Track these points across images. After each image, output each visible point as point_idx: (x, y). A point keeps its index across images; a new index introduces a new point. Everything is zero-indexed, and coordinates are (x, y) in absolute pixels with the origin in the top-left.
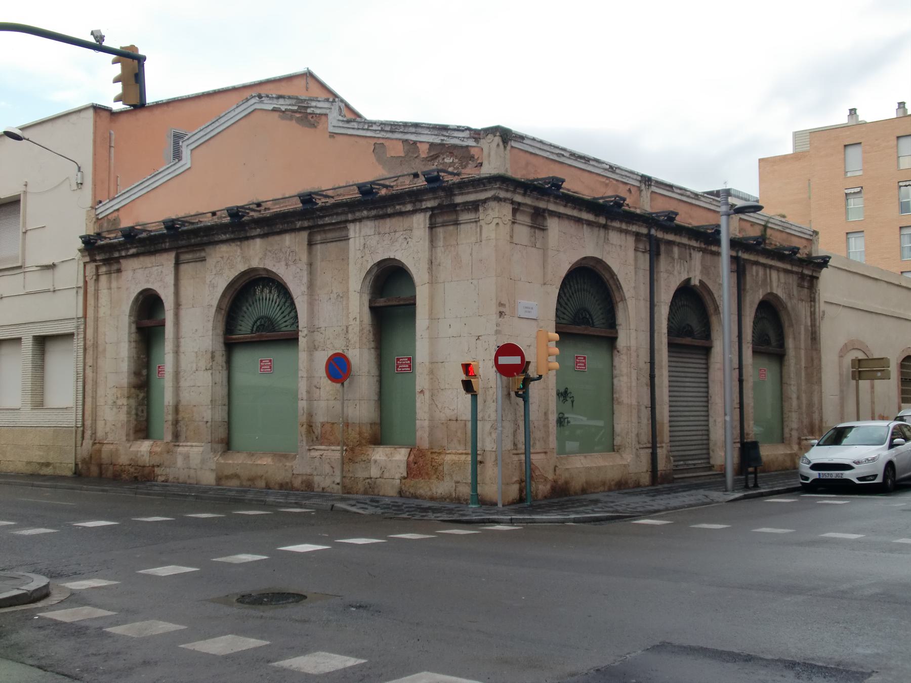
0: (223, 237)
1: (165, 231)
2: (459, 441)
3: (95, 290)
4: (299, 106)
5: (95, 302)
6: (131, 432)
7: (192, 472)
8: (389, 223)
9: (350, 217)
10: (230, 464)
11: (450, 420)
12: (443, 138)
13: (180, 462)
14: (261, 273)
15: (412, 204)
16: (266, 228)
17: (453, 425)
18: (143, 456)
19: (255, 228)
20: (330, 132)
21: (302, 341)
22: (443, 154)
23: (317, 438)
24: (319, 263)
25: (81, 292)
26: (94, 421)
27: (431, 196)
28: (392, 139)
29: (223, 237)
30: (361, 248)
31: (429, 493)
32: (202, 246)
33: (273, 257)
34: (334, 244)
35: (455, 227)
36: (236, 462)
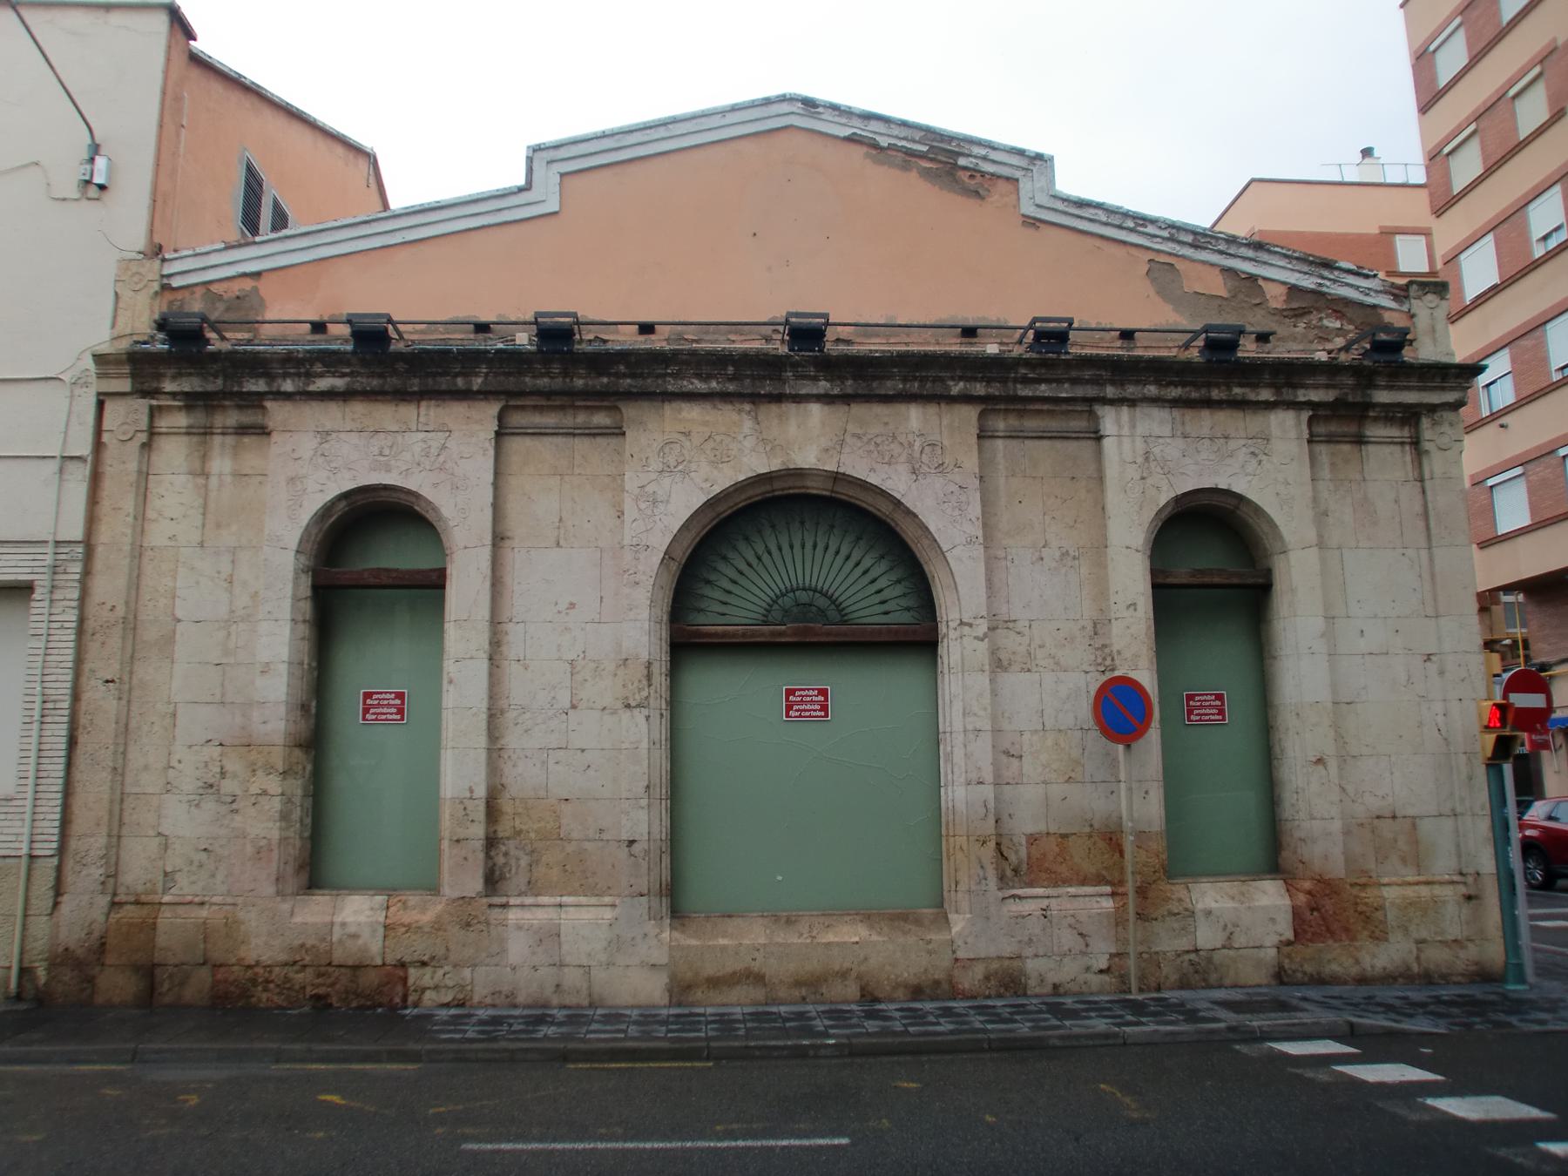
0: (699, 386)
1: (784, 350)
2: (1404, 860)
3: (140, 472)
4: (932, 147)
5: (136, 505)
6: (290, 869)
7: (572, 977)
8: (1206, 420)
9: (1110, 391)
10: (724, 948)
11: (1378, 817)
12: (1319, 281)
13: (518, 949)
14: (809, 484)
15: (1273, 390)
16: (850, 382)
17: (1386, 828)
18: (355, 936)
19: (815, 379)
20: (1023, 216)
21: (957, 648)
22: (1319, 310)
23: (1016, 871)
24: (1002, 481)
25: (81, 473)
26: (114, 840)
27: (1322, 380)
28: (1194, 261)
29: (699, 386)
30: (1140, 460)
31: (1354, 971)
32: (610, 398)
33: (870, 452)
34: (1046, 443)
35: (1355, 448)
36: (746, 942)
